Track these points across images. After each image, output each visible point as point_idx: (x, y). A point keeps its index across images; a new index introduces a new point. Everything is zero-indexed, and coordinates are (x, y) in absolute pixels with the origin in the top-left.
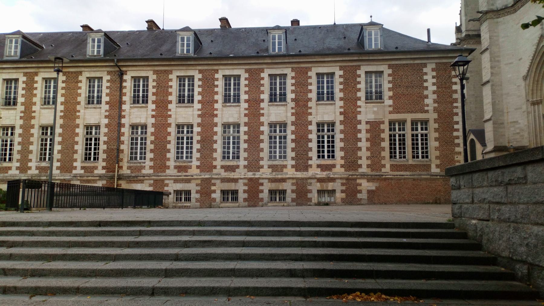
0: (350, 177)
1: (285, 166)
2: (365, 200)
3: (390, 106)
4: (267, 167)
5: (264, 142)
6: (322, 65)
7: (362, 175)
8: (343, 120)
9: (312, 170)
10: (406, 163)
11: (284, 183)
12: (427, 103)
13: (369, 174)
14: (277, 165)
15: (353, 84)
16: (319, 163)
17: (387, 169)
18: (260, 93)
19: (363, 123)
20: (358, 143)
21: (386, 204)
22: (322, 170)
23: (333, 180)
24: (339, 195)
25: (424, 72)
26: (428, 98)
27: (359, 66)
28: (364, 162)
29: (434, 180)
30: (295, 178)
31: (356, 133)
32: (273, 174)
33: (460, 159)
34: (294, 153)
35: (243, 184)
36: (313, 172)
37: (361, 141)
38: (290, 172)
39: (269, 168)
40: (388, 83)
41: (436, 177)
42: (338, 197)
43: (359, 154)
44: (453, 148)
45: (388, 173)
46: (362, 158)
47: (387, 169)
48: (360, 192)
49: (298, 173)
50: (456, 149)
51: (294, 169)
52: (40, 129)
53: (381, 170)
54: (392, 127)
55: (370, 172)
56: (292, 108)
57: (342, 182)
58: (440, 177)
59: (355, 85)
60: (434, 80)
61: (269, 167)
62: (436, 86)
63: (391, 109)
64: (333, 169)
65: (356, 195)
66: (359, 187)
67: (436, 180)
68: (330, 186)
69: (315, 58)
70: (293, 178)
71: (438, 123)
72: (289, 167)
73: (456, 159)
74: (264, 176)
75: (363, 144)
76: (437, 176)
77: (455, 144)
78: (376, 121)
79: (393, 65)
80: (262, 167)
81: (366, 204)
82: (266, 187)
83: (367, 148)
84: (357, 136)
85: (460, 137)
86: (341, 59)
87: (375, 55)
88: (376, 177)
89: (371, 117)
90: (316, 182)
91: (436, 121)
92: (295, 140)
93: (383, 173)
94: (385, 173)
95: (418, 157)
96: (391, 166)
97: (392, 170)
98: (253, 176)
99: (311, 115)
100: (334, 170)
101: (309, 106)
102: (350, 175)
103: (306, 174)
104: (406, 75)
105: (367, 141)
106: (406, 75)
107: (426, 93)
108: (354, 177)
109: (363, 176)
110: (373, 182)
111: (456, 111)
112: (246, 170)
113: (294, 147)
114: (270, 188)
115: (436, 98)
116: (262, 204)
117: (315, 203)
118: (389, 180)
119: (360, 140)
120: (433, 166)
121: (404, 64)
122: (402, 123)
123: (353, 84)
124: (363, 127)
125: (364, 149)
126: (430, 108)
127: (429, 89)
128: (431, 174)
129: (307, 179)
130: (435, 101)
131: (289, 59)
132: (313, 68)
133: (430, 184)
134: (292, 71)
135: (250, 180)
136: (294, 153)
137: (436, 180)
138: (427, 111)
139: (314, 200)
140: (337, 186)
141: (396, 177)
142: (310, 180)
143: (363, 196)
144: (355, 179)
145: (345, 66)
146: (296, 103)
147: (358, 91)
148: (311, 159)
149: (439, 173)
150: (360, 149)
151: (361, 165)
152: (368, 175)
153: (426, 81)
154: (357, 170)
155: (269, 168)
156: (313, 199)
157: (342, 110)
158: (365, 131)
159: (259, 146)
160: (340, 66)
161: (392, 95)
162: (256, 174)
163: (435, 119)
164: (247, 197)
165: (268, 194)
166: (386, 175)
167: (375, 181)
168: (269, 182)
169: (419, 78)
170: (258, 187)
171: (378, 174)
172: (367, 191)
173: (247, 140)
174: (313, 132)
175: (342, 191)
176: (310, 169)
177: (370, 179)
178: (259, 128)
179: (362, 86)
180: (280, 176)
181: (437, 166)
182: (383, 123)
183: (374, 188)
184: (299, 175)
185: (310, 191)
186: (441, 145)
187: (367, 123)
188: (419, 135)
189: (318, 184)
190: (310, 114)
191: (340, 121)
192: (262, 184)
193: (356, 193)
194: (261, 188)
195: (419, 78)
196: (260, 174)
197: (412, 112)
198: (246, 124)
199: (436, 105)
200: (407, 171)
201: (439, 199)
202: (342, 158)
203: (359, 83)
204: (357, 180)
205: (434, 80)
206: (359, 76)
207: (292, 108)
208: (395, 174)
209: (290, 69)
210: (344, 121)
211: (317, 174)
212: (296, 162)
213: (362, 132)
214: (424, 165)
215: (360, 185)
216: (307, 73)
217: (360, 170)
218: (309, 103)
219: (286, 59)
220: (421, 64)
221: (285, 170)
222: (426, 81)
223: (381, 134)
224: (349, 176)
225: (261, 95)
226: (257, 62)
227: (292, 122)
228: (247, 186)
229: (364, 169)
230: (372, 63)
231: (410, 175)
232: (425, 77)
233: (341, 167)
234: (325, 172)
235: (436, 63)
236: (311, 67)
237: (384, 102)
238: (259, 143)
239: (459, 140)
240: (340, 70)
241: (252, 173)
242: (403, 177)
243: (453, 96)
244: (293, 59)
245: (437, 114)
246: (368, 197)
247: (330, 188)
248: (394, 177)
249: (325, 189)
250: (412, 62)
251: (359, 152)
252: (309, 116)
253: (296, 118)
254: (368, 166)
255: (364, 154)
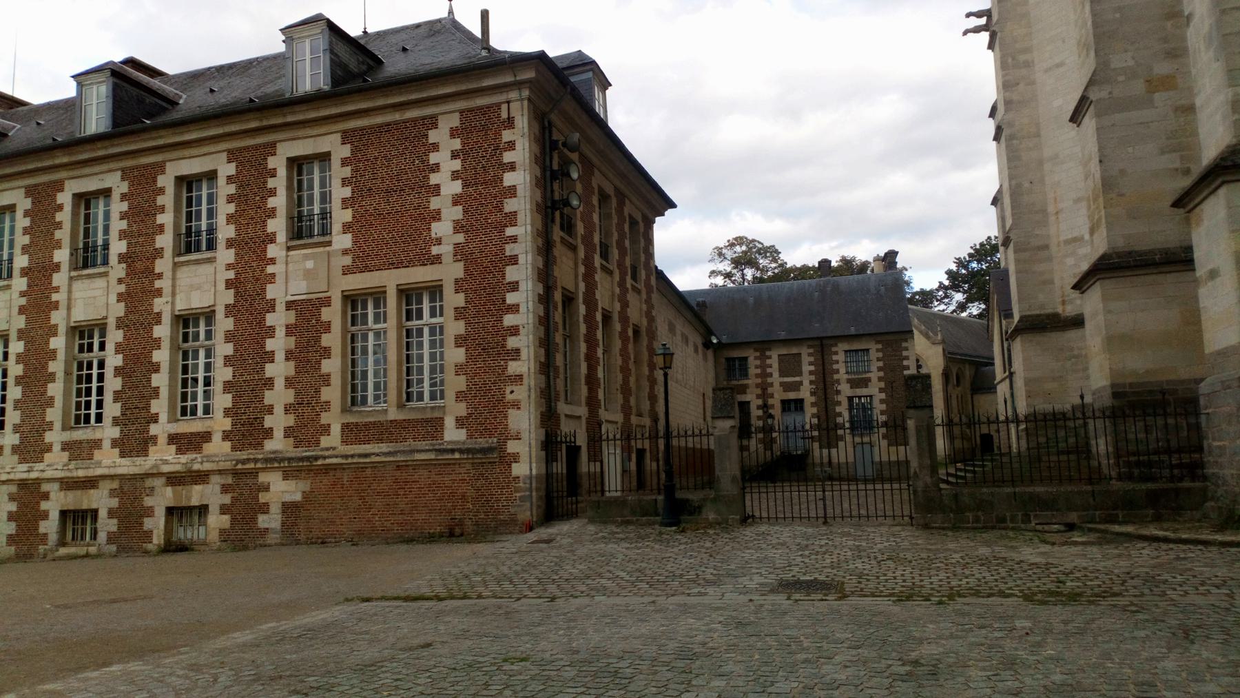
0: (240, 466)
1: (97, 444)
2: (275, 533)
3: (345, 252)
4: (59, 447)
5: (57, 380)
6: (187, 152)
7: (266, 460)
8: (232, 302)
9: (157, 452)
10: (381, 418)
11: (92, 491)
12: (438, 235)
13: (289, 455)
14: (81, 442)
15: (258, 198)
16: (173, 431)
17: (333, 440)
18: (54, 248)
19: (280, 307)
20: (267, 365)
21: (325, 543)
22: (180, 451)
23: (201, 477)
24: (217, 521)
25: (431, 141)
26: (439, 220)
27: (273, 145)
28: (278, 421)
29: (449, 464)
30: (115, 476)
31: (263, 338)
32: (70, 467)
33: (520, 397)
34: (119, 405)
35: (6, 497)
36: (158, 456)
37: (273, 361)
38: (109, 461)
39: (63, 449)
40: (340, 186)
41: (450, 456)
42: (212, 526)
43: (269, 397)
44: (502, 362)
45: (334, 449)
46: (275, 410)
47: (333, 440)
48: (265, 508)
49: (125, 461)
50: (509, 368)
51: (117, 451)
52: (178, 326)
53: (318, 443)
54: (359, 312)
55: (291, 449)
56: (120, 281)
57: (223, 482)
58: (462, 456)
59: (264, 199)
60: (457, 165)
61: (66, 446)
62: (460, 182)
63: (348, 260)
64: (205, 446)
65: (254, 520)
66: (264, 493)
67: (454, 464)
68: (196, 495)
69: (161, 137)
70: (112, 477)
71: (465, 291)
72: (107, 444)
73: (509, 397)
74: (49, 474)
75: (279, 369)
76: (453, 451)
77: (508, 352)
78: (310, 300)
79: (354, 130)
80: (49, 449)
81: (276, 544)
82: (54, 505)
83: (287, 379)
84: (263, 347)
85: (521, 328)
86: (220, 131)
87: (297, 108)
88: (301, 464)
89: (299, 288)
90: (163, 486)
91: (459, 286)
92: (123, 368)
93: (322, 450)
94: (327, 449)
95: (420, 397)
96: (345, 427)
97: (345, 442)
98: (25, 476)
99: (160, 295)
100: (209, 448)
101: (157, 271)
102: (238, 462)
103: (142, 463)
104: (385, 157)
105: (287, 359)
106: (385, 157)
107: (435, 203)
108: (247, 466)
109: (274, 461)
110: (296, 478)
111: (511, 250)
112: (16, 457)
113: (120, 388)
114: (62, 505)
115: (461, 217)
116: (45, 549)
117: (159, 545)
118: (335, 469)
119: (270, 357)
120: (449, 422)
121: (380, 126)
122: (378, 296)
123: (258, 198)
124: (278, 319)
125: (279, 383)
126: (445, 250)
127: (443, 191)
128: (442, 447)
129: (148, 475)
130: (458, 227)
131: (106, 148)
132: (168, 164)
133: (438, 478)
134: (123, 179)
135: (23, 484)
136: (119, 405)
137: (454, 464)
138: (437, 260)
139: (159, 536)
140: (209, 494)
141: (350, 460)
142: (150, 479)
143: (271, 521)
144: (254, 473)
145: (240, 150)
146: (129, 266)
147: (269, 217)
148: (156, 421)
149: (464, 443)
150: (269, 383)
151: (271, 429)
152: (282, 460)
153: (436, 168)
154: (259, 445)
155: (63, 449)
156: (155, 532)
157: (231, 275)
158: (284, 329)
159: (45, 392)
160: (229, 151)
161: (350, 220)
162: (35, 469)
163: (457, 281)
164: (14, 532)
165: (57, 523)
166: (325, 458)
167: (303, 474)
168: (61, 490)
169: (417, 162)
170: (38, 503)
171: (307, 454)
172: (280, 506)
173: (22, 377)
174: (162, 344)
175: (224, 510)
176: (152, 449)
177: (291, 469)
178: (47, 343)
179: (279, 202)
180: (81, 473)
181: (460, 422)
182: (327, 302)
183: (298, 497)
184: (127, 466)
185: (149, 512)
186: (469, 357)
187: (290, 305)
188: (426, 331)
189: (169, 491)
190: (159, 293)
191: (227, 306)
192: (46, 496)
193: (256, 513)
194: (44, 505)
195: (417, 162)
196: (41, 468)
197: (398, 265)
198: (21, 334)
199: (460, 238)
200: (381, 441)
201: (461, 523)
202: (227, 412)
203: (273, 193)
204: (260, 474)
205: (457, 165)
206: (273, 173)
207: (120, 281)
208: (352, 452)
209: (119, 173)
210: (234, 306)
211: (166, 462)
212: (122, 431)
213: (277, 332)
214: (427, 421)
215: (266, 488)
216: (155, 181)
217: (270, 445)
218: (158, 262)
219: (99, 149)
220: (424, 118)
221: (97, 455)
222: (436, 168)
223: (323, 335)
224: (237, 464)
225: (55, 251)
226: (40, 165)
227: (119, 319)
228: (16, 503)
229: (277, 444)
230: (301, 133)
231: (386, 454)
232: (433, 158)
233: (223, 440)
234: (186, 456)
235: (461, 112)
236: (164, 162)
237: (329, 243)
238: (45, 385)
239: (519, 337)
240: (229, 161)
241: (28, 465)
242: (367, 460)
243: (505, 205)
244: (113, 146)
245: (462, 264)
246: (283, 524)
247: (195, 502)
248: (344, 461)
249: (184, 503)
250: (397, 116)
251: (267, 393)
252: (156, 300)
253: (126, 306)
254: (288, 432)
255: (279, 396)
